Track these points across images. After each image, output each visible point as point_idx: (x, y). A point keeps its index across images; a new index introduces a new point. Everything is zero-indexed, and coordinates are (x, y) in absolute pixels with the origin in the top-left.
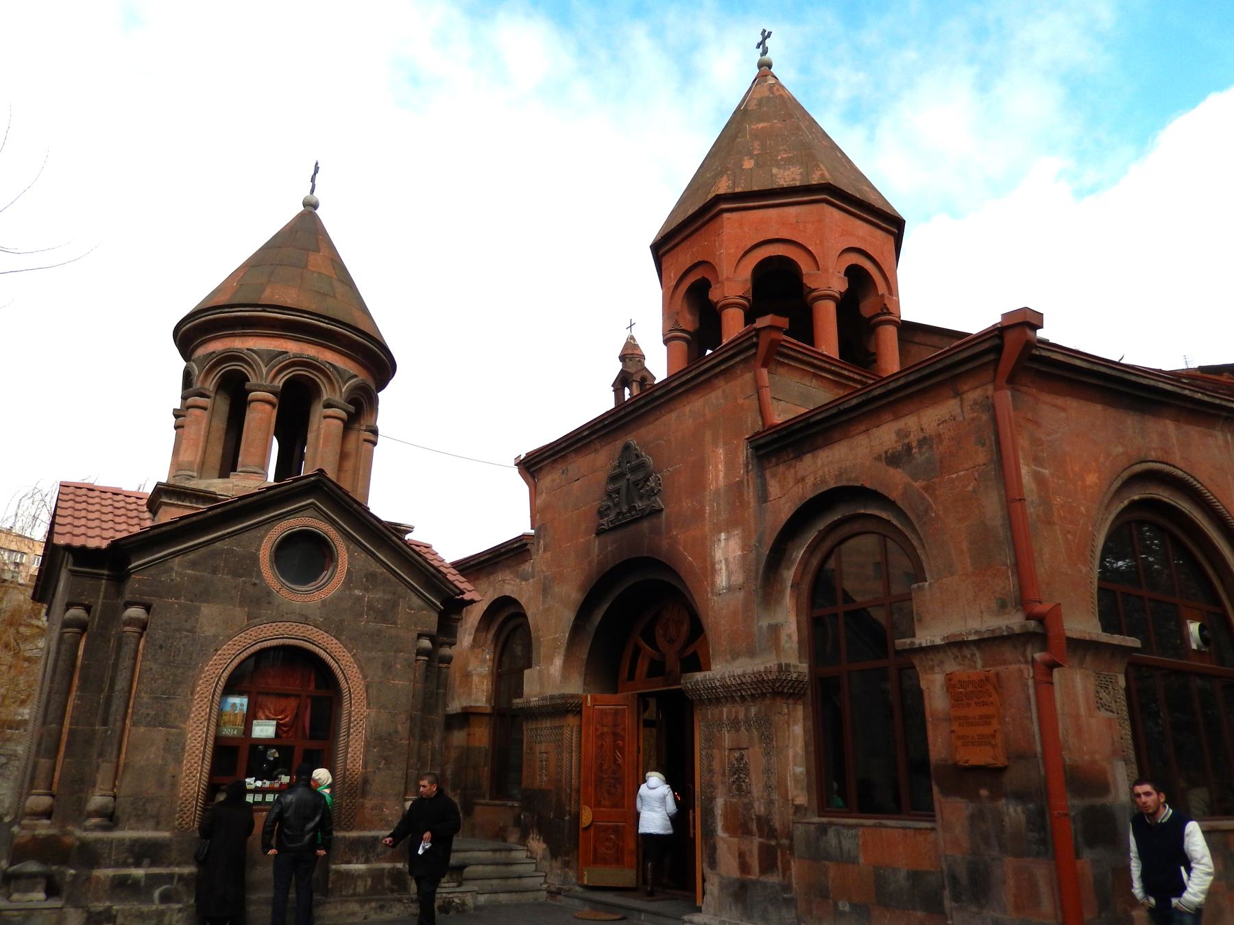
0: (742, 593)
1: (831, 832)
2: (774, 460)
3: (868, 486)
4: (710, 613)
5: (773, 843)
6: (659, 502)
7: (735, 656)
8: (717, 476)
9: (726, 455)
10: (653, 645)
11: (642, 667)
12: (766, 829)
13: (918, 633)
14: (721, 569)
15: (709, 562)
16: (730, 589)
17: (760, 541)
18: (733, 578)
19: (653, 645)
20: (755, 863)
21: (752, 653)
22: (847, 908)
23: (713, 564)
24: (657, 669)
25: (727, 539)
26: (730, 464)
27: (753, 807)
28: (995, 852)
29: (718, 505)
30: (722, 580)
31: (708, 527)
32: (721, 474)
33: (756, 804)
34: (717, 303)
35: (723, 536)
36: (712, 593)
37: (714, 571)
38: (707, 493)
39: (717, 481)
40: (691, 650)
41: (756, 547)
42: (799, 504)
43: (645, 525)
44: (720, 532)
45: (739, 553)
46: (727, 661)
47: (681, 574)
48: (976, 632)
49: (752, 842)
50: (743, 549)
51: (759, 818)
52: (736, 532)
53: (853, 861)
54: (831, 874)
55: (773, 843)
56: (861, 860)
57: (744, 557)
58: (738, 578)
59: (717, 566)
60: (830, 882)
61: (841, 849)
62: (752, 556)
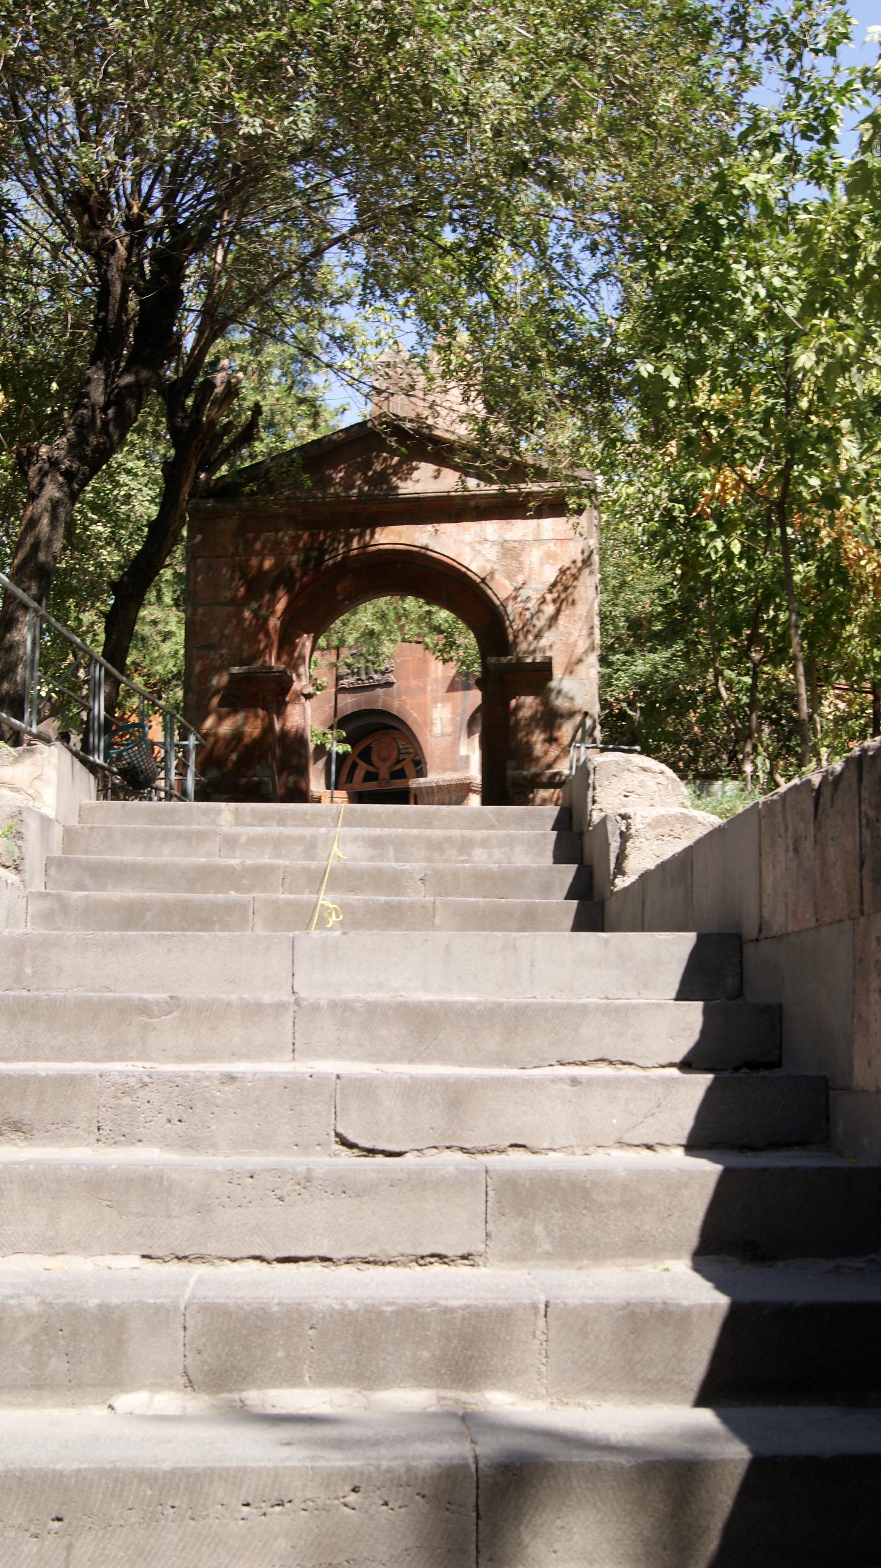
6: (392, 678)
7: (444, 770)
8: (436, 671)
10: (371, 763)
11: (359, 774)
16: (443, 735)
17: (464, 711)
19: (371, 763)
21: (455, 770)
23: (432, 720)
24: (370, 777)
30: (437, 729)
31: (429, 699)
35: (439, 705)
37: (432, 724)
40: (399, 767)
43: (380, 691)
45: (450, 716)
57: (453, 719)
58: (449, 729)
62: (458, 719)
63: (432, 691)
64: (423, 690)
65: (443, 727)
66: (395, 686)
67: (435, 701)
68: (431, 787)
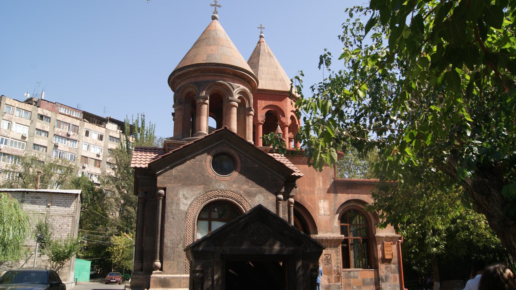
0: (329, 217)
1: (352, 273)
2: (340, 187)
3: (366, 201)
4: (318, 220)
5: (338, 276)
9: (323, 180)
12: (337, 273)
13: (377, 233)
14: (321, 209)
15: (317, 206)
16: (325, 215)
17: (335, 205)
18: (326, 212)
20: (333, 280)
21: (333, 232)
22: (356, 287)
23: (318, 207)
25: (324, 202)
26: (324, 183)
27: (332, 268)
28: (390, 273)
29: (320, 192)
30: (322, 212)
32: (321, 184)
33: (334, 267)
34: (285, 123)
36: (318, 215)
37: (319, 209)
38: (316, 188)
39: (319, 185)
41: (334, 207)
42: (347, 200)
44: (321, 199)
45: (328, 206)
46: (324, 233)
47: (306, 207)
48: (391, 235)
49: (332, 276)
50: (329, 206)
51: (334, 270)
52: (327, 201)
53: (357, 278)
54: (352, 281)
55: (338, 276)
56: (359, 277)
57: (330, 208)
58: (328, 213)
59: (320, 208)
60: (351, 283)
61: (354, 276)
62: (333, 208)
63: (317, 194)
64: (313, 192)
65: (325, 211)
66: (297, 188)
67: (320, 198)
68: (323, 240)
